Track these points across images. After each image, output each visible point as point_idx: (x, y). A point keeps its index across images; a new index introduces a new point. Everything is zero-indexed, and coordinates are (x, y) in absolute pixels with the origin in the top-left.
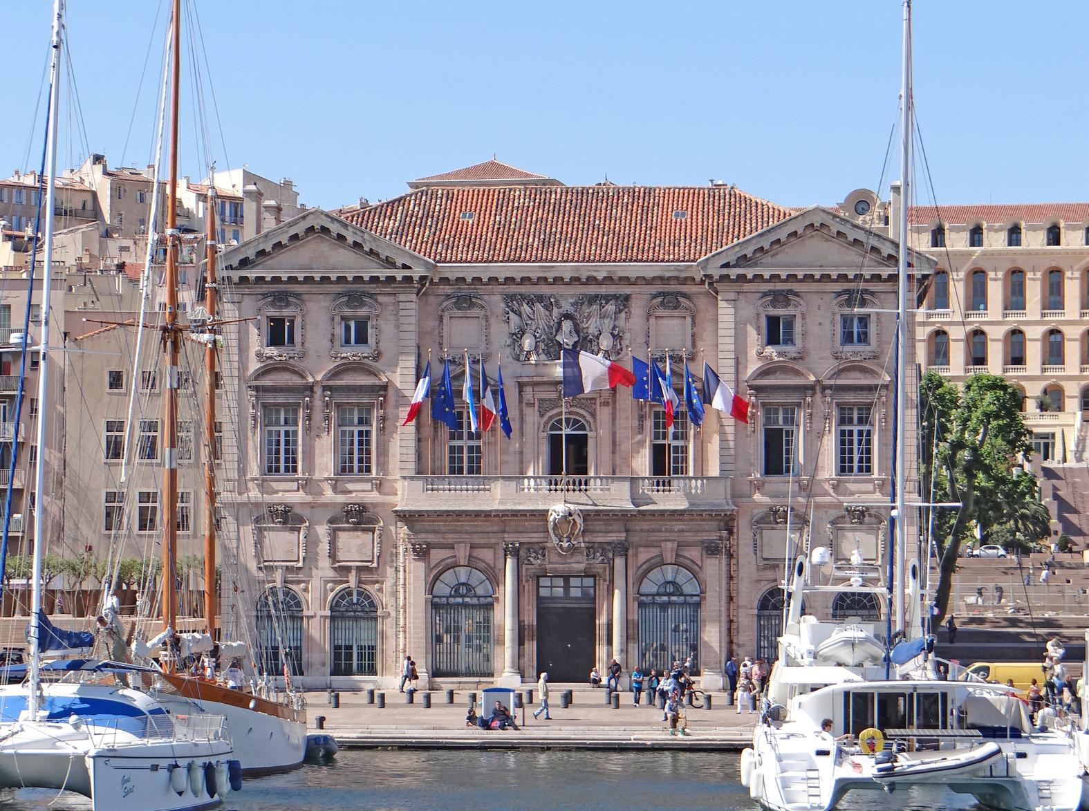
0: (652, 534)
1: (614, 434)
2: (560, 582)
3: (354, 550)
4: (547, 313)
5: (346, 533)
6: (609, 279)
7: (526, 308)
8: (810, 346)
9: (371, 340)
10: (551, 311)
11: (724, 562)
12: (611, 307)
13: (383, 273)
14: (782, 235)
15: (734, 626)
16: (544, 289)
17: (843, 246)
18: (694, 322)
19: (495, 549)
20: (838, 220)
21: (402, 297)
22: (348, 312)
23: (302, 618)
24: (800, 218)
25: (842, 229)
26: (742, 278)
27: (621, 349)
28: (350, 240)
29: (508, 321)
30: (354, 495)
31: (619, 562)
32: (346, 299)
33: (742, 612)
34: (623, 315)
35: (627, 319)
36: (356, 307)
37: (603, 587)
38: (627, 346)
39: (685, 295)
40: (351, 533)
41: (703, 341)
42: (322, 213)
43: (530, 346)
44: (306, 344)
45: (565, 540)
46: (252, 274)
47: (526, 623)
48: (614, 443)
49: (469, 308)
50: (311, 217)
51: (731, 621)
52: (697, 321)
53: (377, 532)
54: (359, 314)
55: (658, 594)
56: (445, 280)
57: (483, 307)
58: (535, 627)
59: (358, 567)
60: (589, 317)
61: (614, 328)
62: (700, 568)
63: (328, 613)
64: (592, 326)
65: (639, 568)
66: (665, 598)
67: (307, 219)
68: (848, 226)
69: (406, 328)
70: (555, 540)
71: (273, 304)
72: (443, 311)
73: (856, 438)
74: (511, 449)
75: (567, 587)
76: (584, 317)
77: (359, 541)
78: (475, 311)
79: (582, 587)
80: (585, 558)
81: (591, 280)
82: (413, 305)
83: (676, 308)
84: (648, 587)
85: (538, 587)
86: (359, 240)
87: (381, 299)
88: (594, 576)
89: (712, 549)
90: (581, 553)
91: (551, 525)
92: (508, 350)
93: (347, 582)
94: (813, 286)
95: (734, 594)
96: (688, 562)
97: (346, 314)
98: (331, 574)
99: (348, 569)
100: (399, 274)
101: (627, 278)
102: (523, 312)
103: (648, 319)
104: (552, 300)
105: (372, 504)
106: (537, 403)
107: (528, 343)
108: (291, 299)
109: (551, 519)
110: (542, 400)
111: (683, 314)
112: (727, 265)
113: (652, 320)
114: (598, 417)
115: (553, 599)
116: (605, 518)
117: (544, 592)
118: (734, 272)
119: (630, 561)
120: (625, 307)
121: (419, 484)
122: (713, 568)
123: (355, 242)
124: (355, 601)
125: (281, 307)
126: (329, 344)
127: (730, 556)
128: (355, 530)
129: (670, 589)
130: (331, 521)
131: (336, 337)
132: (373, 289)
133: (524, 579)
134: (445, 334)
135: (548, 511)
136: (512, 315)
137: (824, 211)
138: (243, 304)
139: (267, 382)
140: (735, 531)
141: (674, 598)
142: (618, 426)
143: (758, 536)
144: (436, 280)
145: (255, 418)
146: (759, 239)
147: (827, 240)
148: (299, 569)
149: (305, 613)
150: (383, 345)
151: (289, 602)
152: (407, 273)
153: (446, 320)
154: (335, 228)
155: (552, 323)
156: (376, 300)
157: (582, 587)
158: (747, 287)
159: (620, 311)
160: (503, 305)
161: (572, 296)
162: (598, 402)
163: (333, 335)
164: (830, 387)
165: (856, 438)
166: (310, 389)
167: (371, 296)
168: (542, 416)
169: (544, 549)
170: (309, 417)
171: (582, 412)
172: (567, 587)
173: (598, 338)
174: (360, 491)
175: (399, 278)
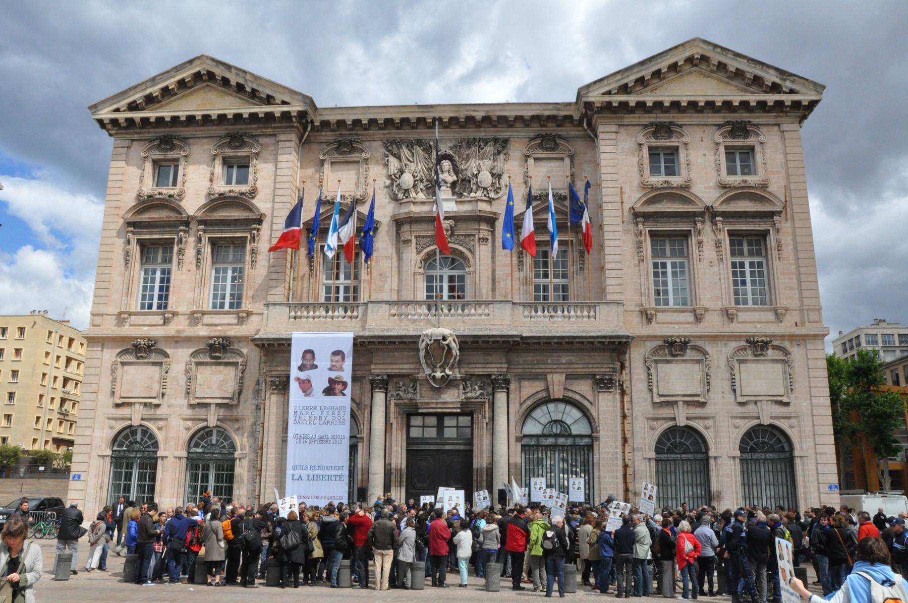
0: (536, 366)
1: (494, 271)
2: (433, 421)
3: (215, 387)
4: (427, 156)
5: (208, 368)
6: (487, 119)
7: (405, 152)
8: (694, 176)
9: (251, 178)
10: (430, 154)
11: (618, 397)
12: (490, 149)
13: (262, 110)
14: (663, 65)
15: (630, 471)
16: (422, 133)
17: (723, 82)
18: (572, 162)
19: (362, 383)
20: (719, 50)
21: (282, 137)
22: (229, 152)
23: (156, 459)
24: (681, 48)
25: (723, 60)
26: (624, 105)
27: (500, 188)
28: (233, 83)
29: (386, 165)
30: (218, 328)
31: (501, 397)
32: (228, 140)
33: (638, 456)
34: (502, 156)
36: (236, 147)
37: (482, 421)
39: (560, 137)
40: (214, 367)
42: (208, 57)
44: (186, 184)
45: (439, 370)
46: (137, 115)
47: (393, 466)
48: (494, 280)
49: (350, 152)
50: (198, 62)
51: (626, 466)
52: (576, 162)
53: (240, 367)
54: (239, 154)
55: (543, 436)
56: (325, 124)
58: (404, 471)
59: (217, 405)
60: (467, 159)
61: (493, 169)
62: (591, 403)
63: (185, 454)
64: (472, 166)
65: (521, 404)
66: (550, 441)
67: (195, 64)
68: (730, 56)
70: (428, 371)
71: (158, 147)
73: (747, 269)
74: (387, 286)
75: (440, 427)
76: (463, 159)
77: (221, 377)
78: (355, 156)
79: (457, 427)
80: (461, 391)
81: (470, 120)
82: (292, 144)
83: (553, 149)
84: (532, 428)
85: (408, 427)
86: (242, 81)
87: (263, 140)
88: (471, 414)
89: (603, 383)
90: (457, 386)
91: (422, 354)
93: (206, 420)
94: (696, 118)
95: (628, 435)
96: (578, 398)
97: (227, 154)
98: (189, 412)
99: (206, 405)
100: (277, 110)
101: (505, 117)
102: (402, 155)
103: (526, 161)
104: (431, 143)
105: (235, 337)
106: (414, 241)
107: (407, 179)
108: (175, 142)
109: (422, 346)
110: (419, 237)
111: (561, 156)
112: (609, 93)
113: (531, 161)
114: (477, 253)
115: (423, 441)
116: (484, 345)
117: (415, 433)
118: (616, 99)
119: (511, 396)
122: (606, 406)
123: (237, 83)
124: (214, 442)
125: (166, 150)
126: (209, 184)
127: (623, 393)
128: (219, 364)
129: (556, 430)
130: (194, 355)
131: (216, 175)
132: (253, 129)
133: (392, 416)
135: (419, 337)
136: (392, 159)
137: (705, 42)
138: (132, 149)
139: (146, 217)
140: (627, 364)
141: (561, 441)
142: (497, 263)
143: (653, 371)
144: (317, 124)
145: (127, 254)
146: (640, 68)
147: (706, 76)
148: (157, 406)
149: (159, 454)
150: (259, 184)
151: (146, 442)
152: (285, 108)
154: (219, 72)
155: (431, 165)
156: (257, 141)
157: (457, 427)
158: (628, 119)
159: (499, 153)
160: (383, 150)
161: (451, 140)
163: (213, 174)
164: (725, 214)
165: (747, 269)
166: (187, 223)
167: (253, 136)
168: (419, 252)
169: (415, 380)
170: (181, 252)
171: (461, 248)
172: (440, 427)
173: (476, 176)
174: (224, 325)
175: (278, 115)
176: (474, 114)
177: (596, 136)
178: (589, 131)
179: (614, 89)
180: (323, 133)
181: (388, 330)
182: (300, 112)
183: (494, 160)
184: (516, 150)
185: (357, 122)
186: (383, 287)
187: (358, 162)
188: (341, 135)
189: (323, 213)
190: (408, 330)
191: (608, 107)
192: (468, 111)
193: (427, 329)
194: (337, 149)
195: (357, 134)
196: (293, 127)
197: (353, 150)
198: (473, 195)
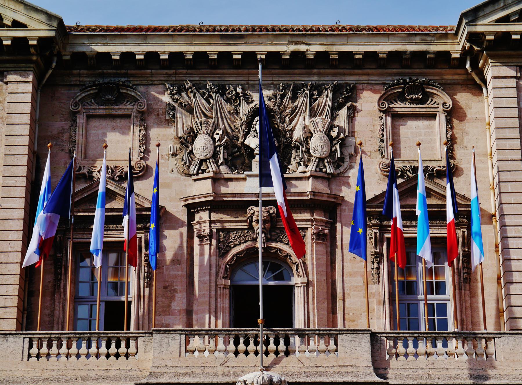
34: (344, 112)
35: (351, 118)
38: (351, 156)
41: (465, 148)
43: (205, 148)
57: (136, 100)
61: (331, 127)
69: (16, 119)
72: (76, 104)
78: (127, 107)
92: (173, 162)
120: (347, 99)
121: (18, 344)
134: (80, 139)
152: (19, 33)
153: (81, 120)
159: (340, 106)
162: (309, 233)
176: (302, 48)
177: (484, 81)
178: (474, 76)
179: (514, 14)
180: (75, 72)
181: (185, 374)
182: (41, 40)
183: (333, 117)
184: (368, 102)
185: (128, 56)
186: (169, 306)
187: (129, 116)
188: (103, 75)
189: (75, 194)
190: (216, 375)
191: (504, 38)
192: (297, 43)
193: (244, 373)
194: (96, 97)
195: (126, 75)
196: (32, 62)
197: (121, 98)
198: (301, 168)
